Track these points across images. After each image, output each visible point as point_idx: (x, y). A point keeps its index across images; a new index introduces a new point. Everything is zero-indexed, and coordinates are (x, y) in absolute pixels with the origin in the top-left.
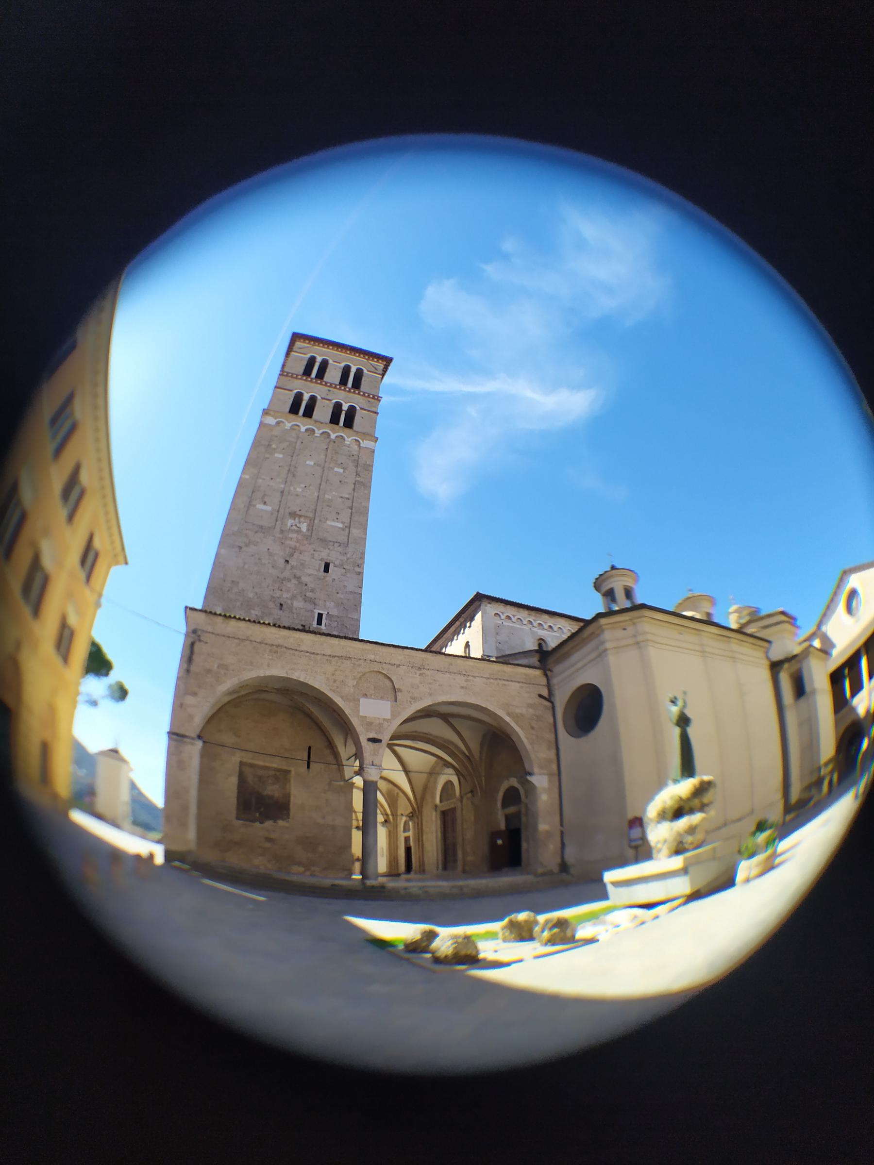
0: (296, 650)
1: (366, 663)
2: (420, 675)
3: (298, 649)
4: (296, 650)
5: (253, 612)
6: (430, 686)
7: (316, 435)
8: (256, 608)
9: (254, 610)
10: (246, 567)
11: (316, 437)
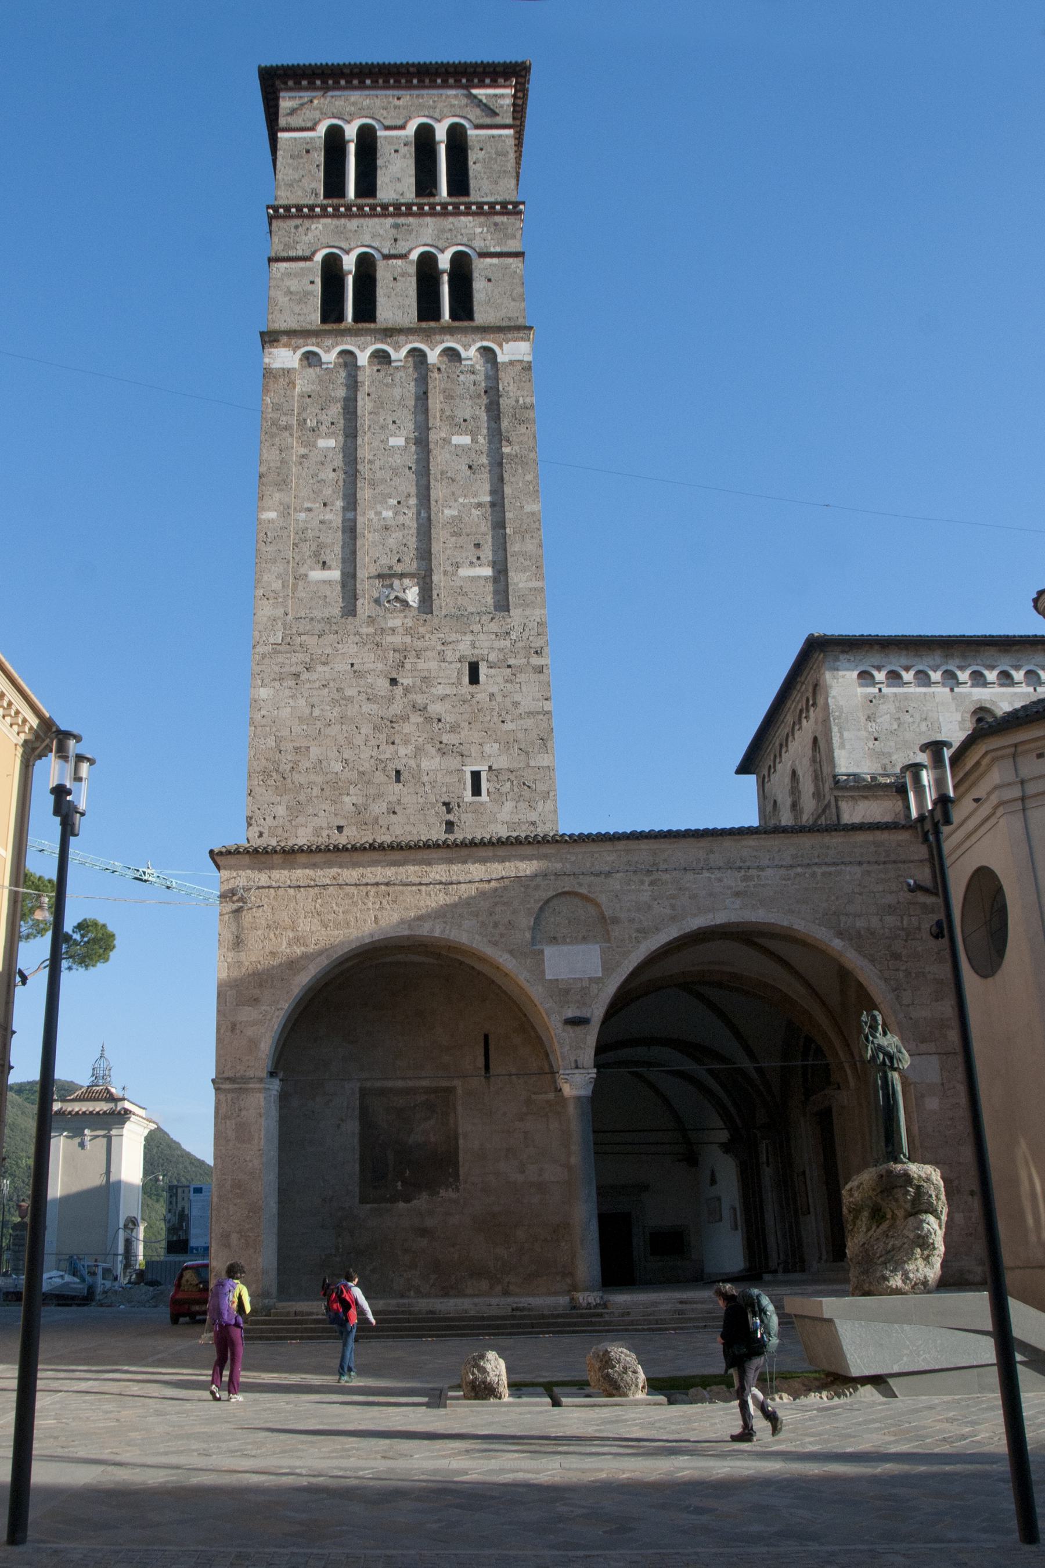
0: (421, 884)
1: (547, 882)
2: (652, 883)
3: (425, 880)
4: (421, 884)
5: (346, 799)
6: (674, 901)
8: (352, 790)
9: (348, 794)
10: (316, 712)
11: (397, 368)
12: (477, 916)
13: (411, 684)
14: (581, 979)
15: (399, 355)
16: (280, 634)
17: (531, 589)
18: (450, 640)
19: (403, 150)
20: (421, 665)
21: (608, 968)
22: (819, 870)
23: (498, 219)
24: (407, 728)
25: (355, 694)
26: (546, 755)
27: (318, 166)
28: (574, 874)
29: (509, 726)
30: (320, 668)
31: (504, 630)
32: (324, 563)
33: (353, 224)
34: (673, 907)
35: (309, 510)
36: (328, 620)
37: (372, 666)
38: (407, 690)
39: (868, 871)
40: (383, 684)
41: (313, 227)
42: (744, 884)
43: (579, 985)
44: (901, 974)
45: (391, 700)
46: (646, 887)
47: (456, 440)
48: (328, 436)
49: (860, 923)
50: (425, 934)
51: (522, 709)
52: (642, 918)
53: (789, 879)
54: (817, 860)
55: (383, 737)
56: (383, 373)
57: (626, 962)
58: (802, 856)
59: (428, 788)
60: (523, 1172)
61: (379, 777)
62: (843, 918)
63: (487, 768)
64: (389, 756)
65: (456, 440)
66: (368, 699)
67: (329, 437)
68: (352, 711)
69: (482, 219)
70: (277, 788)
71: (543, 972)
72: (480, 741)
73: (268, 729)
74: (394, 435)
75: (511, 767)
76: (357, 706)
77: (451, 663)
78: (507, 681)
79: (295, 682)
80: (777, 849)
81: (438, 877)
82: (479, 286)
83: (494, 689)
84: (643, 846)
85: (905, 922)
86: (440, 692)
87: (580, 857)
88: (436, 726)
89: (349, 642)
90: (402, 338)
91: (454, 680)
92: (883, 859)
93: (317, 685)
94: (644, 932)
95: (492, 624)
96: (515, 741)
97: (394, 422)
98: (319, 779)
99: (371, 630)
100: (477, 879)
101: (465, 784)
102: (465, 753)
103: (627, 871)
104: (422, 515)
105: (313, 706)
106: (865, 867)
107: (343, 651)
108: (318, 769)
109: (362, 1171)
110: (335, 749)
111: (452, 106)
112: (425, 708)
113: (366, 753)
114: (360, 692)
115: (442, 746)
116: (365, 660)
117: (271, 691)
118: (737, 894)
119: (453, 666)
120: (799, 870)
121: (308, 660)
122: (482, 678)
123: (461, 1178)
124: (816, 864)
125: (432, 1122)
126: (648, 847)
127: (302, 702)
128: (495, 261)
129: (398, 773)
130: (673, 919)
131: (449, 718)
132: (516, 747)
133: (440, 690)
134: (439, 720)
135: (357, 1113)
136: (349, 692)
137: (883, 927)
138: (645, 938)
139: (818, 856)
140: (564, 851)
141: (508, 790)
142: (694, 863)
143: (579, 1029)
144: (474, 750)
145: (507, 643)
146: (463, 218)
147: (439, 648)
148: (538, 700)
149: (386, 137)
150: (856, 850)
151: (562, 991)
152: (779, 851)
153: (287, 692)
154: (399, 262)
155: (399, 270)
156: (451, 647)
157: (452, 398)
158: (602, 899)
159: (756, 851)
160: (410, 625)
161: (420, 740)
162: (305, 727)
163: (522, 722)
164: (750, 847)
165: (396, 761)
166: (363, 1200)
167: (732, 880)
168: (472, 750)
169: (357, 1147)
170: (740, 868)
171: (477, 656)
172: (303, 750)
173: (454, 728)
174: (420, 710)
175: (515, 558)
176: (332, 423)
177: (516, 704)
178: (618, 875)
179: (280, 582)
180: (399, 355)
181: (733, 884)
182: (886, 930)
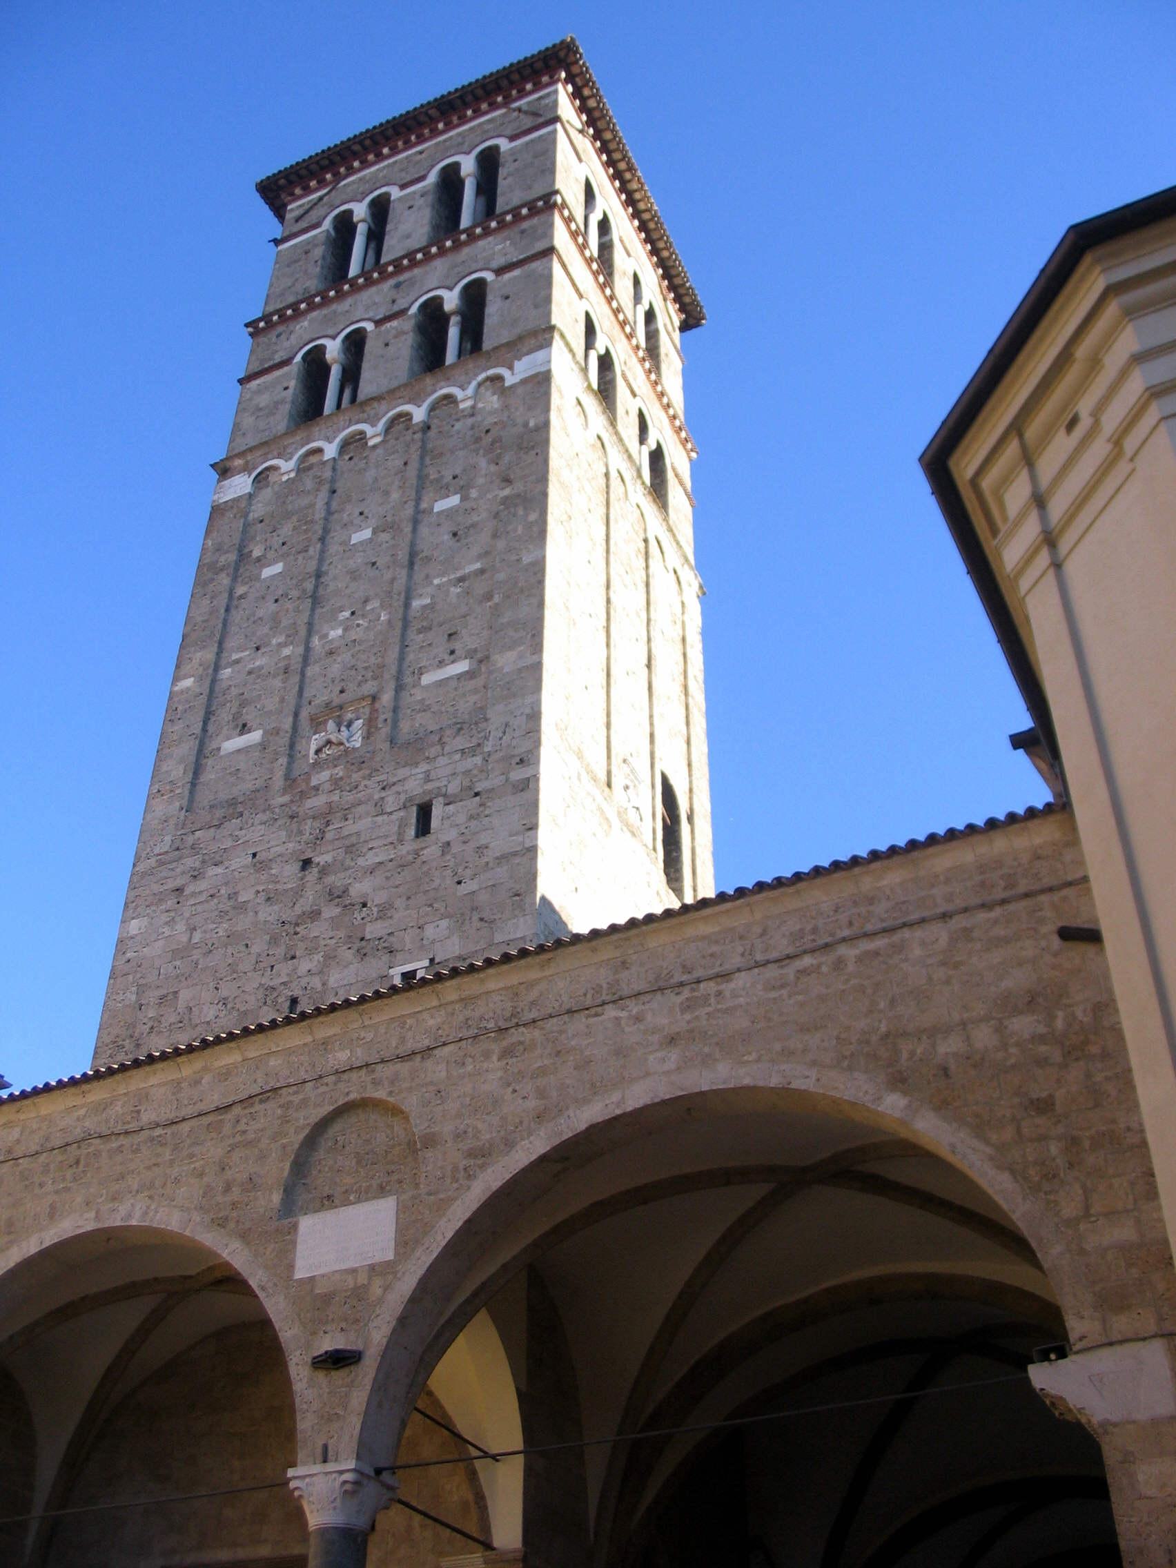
2: (507, 1053)
7: (371, 443)
10: (197, 937)
11: (375, 447)
12: (201, 1175)
14: (354, 1271)
15: (374, 433)
16: (168, 839)
17: (520, 670)
18: (395, 780)
19: (420, 202)
20: (350, 828)
21: (406, 1241)
22: (849, 952)
23: (525, 225)
24: (316, 929)
25: (252, 896)
26: (522, 920)
27: (316, 262)
30: (212, 871)
31: (474, 742)
32: (244, 725)
33: (345, 305)
34: (541, 1093)
35: (237, 662)
36: (233, 803)
37: (279, 849)
38: (324, 871)
39: (965, 929)
40: (293, 868)
41: (298, 327)
42: (688, 1016)
44: (1054, 1149)
45: (299, 892)
47: (441, 506)
48: (275, 562)
49: (949, 1047)
51: (489, 856)
52: (480, 1125)
53: (782, 986)
54: (846, 933)
55: (280, 951)
56: (355, 459)
57: (442, 1222)
58: (815, 930)
63: (426, 963)
65: (441, 506)
67: (277, 563)
68: (243, 923)
69: (506, 233)
71: (291, 1267)
72: (421, 922)
73: (131, 977)
74: (360, 528)
77: (391, 813)
78: (471, 817)
79: (176, 900)
80: (759, 931)
82: (493, 310)
83: (451, 835)
84: (492, 985)
85: (1059, 1024)
86: (369, 862)
89: (257, 822)
90: (384, 406)
91: (393, 838)
92: (999, 894)
94: (482, 1155)
95: (458, 738)
96: (474, 909)
97: (361, 514)
99: (286, 799)
100: (212, 1107)
103: (461, 1040)
104: (382, 618)
105: (194, 929)
106: (958, 922)
107: (245, 839)
111: (487, 131)
114: (258, 892)
115: (364, 943)
116: (273, 843)
118: (672, 1040)
119: (394, 817)
120: (807, 961)
121: (197, 864)
122: (435, 823)
124: (844, 940)
126: (501, 985)
127: (181, 927)
128: (516, 272)
130: (539, 1117)
132: (476, 917)
133: (371, 859)
134: (364, 905)
136: (241, 899)
137: (1004, 1046)
138: (482, 1167)
139: (850, 924)
143: (339, 1376)
144: (408, 939)
145: (478, 760)
146: (481, 243)
147: (376, 797)
148: (516, 834)
149: (400, 199)
150: (935, 891)
153: (165, 918)
154: (395, 323)
155: (394, 332)
156: (394, 789)
157: (441, 454)
158: (411, 1103)
159: (717, 942)
160: (341, 774)
161: (334, 941)
164: (704, 938)
165: (293, 985)
168: (407, 939)
170: (682, 984)
171: (430, 792)
172: (170, 997)
173: (384, 912)
174: (339, 897)
175: (502, 633)
176: (283, 544)
177: (481, 850)
178: (447, 1049)
179: (181, 768)
180: (374, 433)
182: (1013, 1050)
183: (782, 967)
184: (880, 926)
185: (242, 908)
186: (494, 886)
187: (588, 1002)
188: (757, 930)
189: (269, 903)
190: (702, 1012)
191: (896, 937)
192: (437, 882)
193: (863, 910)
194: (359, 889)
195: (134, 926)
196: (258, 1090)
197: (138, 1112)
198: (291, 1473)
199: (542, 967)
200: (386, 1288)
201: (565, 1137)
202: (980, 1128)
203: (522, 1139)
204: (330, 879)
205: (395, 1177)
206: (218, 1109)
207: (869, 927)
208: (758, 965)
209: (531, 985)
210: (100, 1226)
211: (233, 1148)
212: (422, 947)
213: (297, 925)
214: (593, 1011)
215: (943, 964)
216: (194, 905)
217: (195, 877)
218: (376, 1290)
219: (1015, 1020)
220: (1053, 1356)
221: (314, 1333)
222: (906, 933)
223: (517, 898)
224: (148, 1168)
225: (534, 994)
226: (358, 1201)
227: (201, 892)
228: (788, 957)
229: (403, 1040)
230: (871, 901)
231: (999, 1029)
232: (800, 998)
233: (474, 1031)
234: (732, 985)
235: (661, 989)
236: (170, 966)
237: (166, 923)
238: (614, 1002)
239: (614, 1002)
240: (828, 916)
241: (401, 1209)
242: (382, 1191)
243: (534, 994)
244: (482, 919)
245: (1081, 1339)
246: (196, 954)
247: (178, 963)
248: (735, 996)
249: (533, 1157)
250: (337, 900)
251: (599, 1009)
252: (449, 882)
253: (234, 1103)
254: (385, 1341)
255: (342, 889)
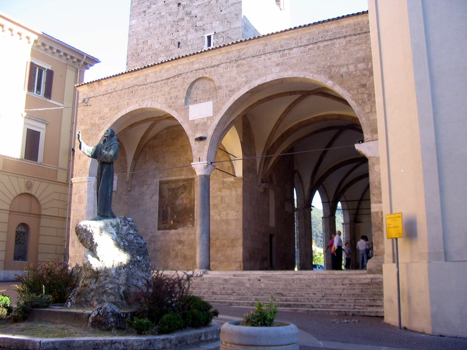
2: (238, 66)
6: (246, 74)
10: (151, 25)
12: (164, 95)
13: (186, 4)
14: (203, 118)
21: (215, 112)
22: (321, 45)
24: (183, 23)
28: (203, 68)
29: (222, 13)
30: (153, 6)
34: (246, 77)
42: (282, 59)
43: (203, 121)
44: (365, 96)
45: (177, 13)
46: (235, 69)
49: (343, 70)
50: (145, 107)
52: (232, 84)
53: (305, 52)
54: (321, 40)
55: (174, 29)
58: (313, 38)
59: (190, 47)
60: (220, 215)
61: (172, 47)
62: (333, 70)
63: (214, 33)
64: (176, 37)
66: (170, 15)
68: (163, 21)
70: (136, 60)
71: (188, 118)
72: (212, 22)
73: (134, 36)
75: (223, 31)
76: (165, 19)
81: (150, 81)
84: (233, 49)
86: (196, 5)
87: (207, 59)
88: (195, 19)
93: (152, 14)
94: (233, 91)
98: (150, 53)
100: (165, 78)
101: (204, 42)
102: (205, 28)
103: (226, 63)
105: (150, 23)
106: (348, 39)
108: (151, 48)
109: (159, 216)
110: (157, 39)
112: (191, 13)
113: (168, 38)
117: (136, 21)
118: (278, 65)
121: (149, 4)
123: (195, 218)
124: (320, 41)
125: (185, 194)
126: (236, 49)
127: (146, 22)
129: (179, 43)
130: (246, 82)
131: (199, 15)
132: (226, 21)
134: (196, 17)
135: (158, 192)
136: (162, 14)
137: (356, 70)
138: (233, 94)
140: (200, 58)
141: (222, 41)
142: (258, 52)
143: (202, 142)
144: (208, 26)
150: (343, 30)
151: (196, 126)
152: (301, 38)
158: (215, 78)
159: (289, 40)
161: (188, 27)
162: (147, 32)
163: (229, 9)
165: (178, 39)
166: (159, 229)
167: (276, 58)
168: (208, 26)
169: (158, 206)
170: (280, 51)
172: (146, 42)
174: (189, 14)
181: (276, 60)
182: (358, 72)
183: (305, 48)
184: (329, 38)
185: (162, 17)
186: (230, 12)
187: (258, 54)
188: (299, 37)
189: (170, 16)
190: (285, 58)
191: (333, 42)
192: (215, 11)
193: (325, 34)
194: (194, 12)
195: (133, 22)
196: (176, 74)
197: (146, 79)
198: (192, 164)
199: (246, 45)
200: (211, 123)
201: (252, 88)
202: (349, 90)
203: (242, 88)
204: (186, 9)
205: (212, 96)
206: (167, 79)
207: (326, 38)
208: (299, 47)
209: (243, 49)
210: (140, 107)
211: (171, 88)
212: (212, 29)
213: (178, 22)
214: (259, 56)
215: (344, 49)
216: (150, 16)
217: (149, 8)
218: (209, 123)
219: (359, 64)
220: (361, 142)
221: (195, 133)
222: (335, 40)
223: (237, 16)
224: (151, 93)
225: (244, 51)
226: (203, 102)
227: (151, 12)
228: (306, 45)
229: (212, 62)
230: (327, 32)
231: (356, 66)
232: (309, 56)
233: (229, 61)
234: (293, 51)
235: (275, 52)
236: (145, 34)
237: (142, 21)
238: (264, 54)
239: (264, 54)
240: (317, 35)
241: (214, 104)
242: (209, 99)
243: (244, 51)
244: (228, 22)
245: (367, 139)
246: (151, 30)
247: (147, 32)
248: (293, 54)
249: (245, 92)
250: (188, 15)
251: (260, 56)
252: (219, 11)
253: (171, 77)
254: (212, 135)
255: (189, 12)
